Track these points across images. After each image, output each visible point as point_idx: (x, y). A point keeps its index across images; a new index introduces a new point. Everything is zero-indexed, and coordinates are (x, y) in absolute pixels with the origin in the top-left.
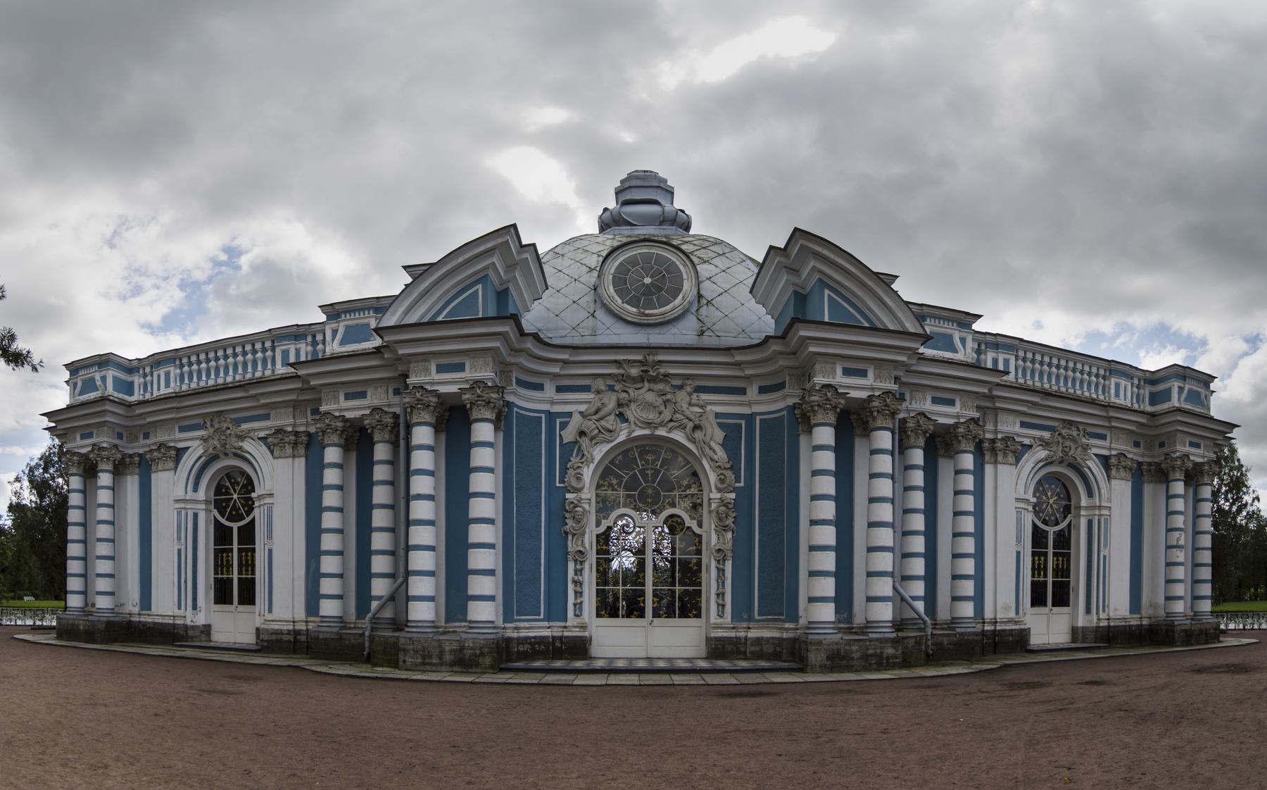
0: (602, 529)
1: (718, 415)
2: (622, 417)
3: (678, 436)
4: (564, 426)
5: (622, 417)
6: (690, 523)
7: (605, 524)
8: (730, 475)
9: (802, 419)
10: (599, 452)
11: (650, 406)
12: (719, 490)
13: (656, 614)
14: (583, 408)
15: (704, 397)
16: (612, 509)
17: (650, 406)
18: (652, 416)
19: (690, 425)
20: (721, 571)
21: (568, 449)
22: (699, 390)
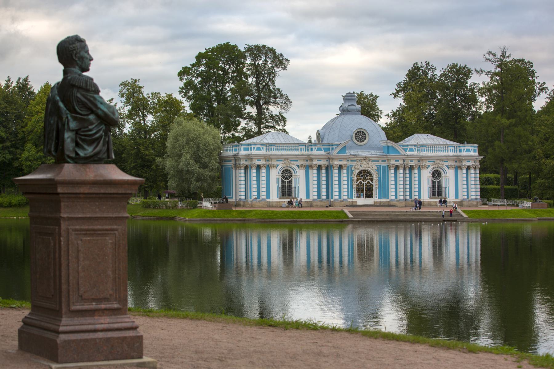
0: (357, 184)
1: (376, 165)
2: (361, 166)
3: (369, 169)
4: (352, 167)
5: (361, 166)
6: (371, 182)
7: (358, 183)
8: (377, 175)
9: (389, 167)
10: (357, 172)
11: (365, 164)
12: (376, 178)
13: (366, 197)
14: (355, 164)
15: (373, 162)
16: (358, 180)
17: (365, 164)
18: (365, 166)
19: (371, 167)
20: (376, 191)
21: (352, 171)
22: (372, 161)
